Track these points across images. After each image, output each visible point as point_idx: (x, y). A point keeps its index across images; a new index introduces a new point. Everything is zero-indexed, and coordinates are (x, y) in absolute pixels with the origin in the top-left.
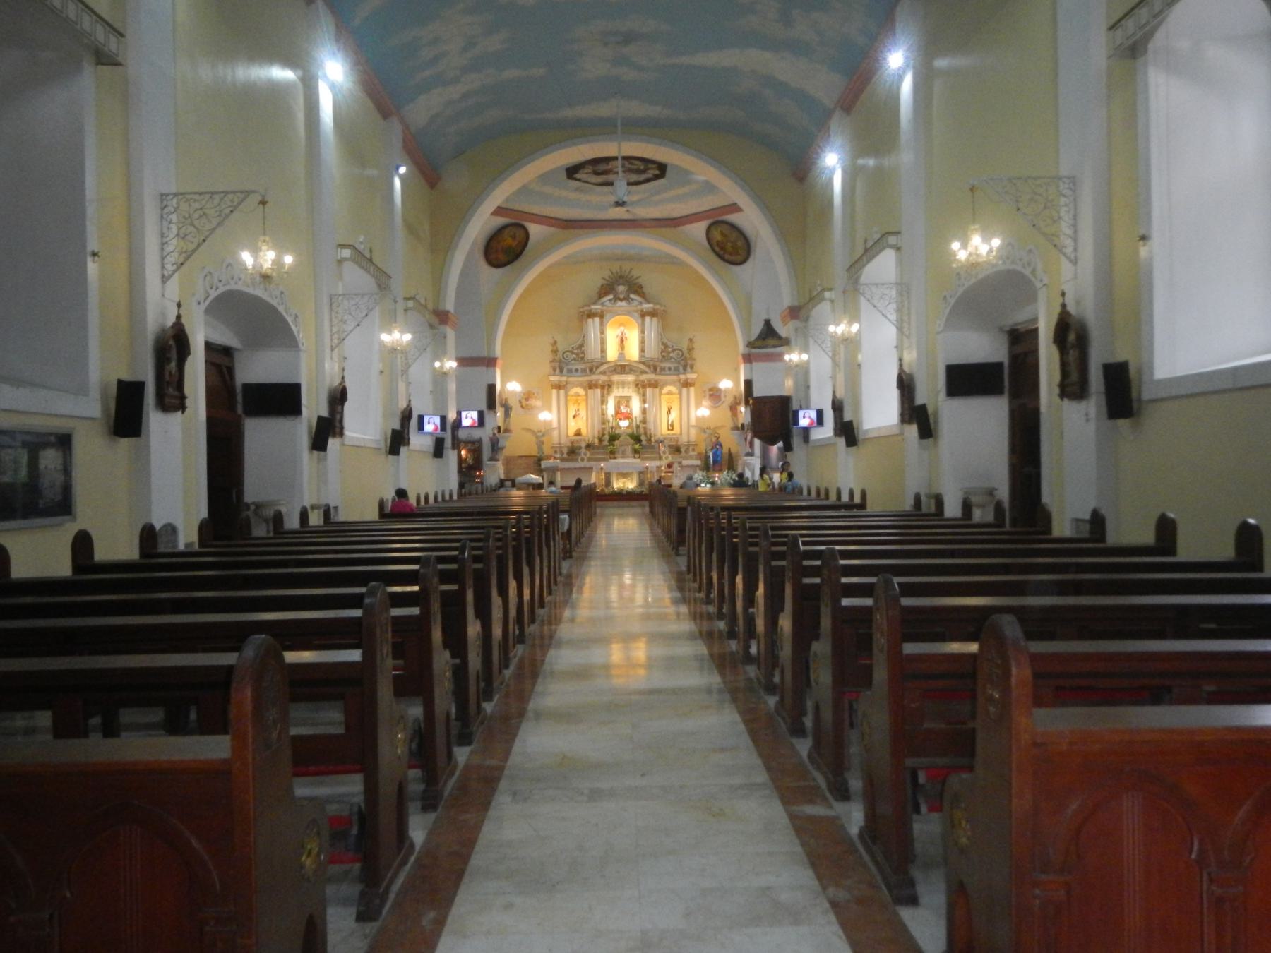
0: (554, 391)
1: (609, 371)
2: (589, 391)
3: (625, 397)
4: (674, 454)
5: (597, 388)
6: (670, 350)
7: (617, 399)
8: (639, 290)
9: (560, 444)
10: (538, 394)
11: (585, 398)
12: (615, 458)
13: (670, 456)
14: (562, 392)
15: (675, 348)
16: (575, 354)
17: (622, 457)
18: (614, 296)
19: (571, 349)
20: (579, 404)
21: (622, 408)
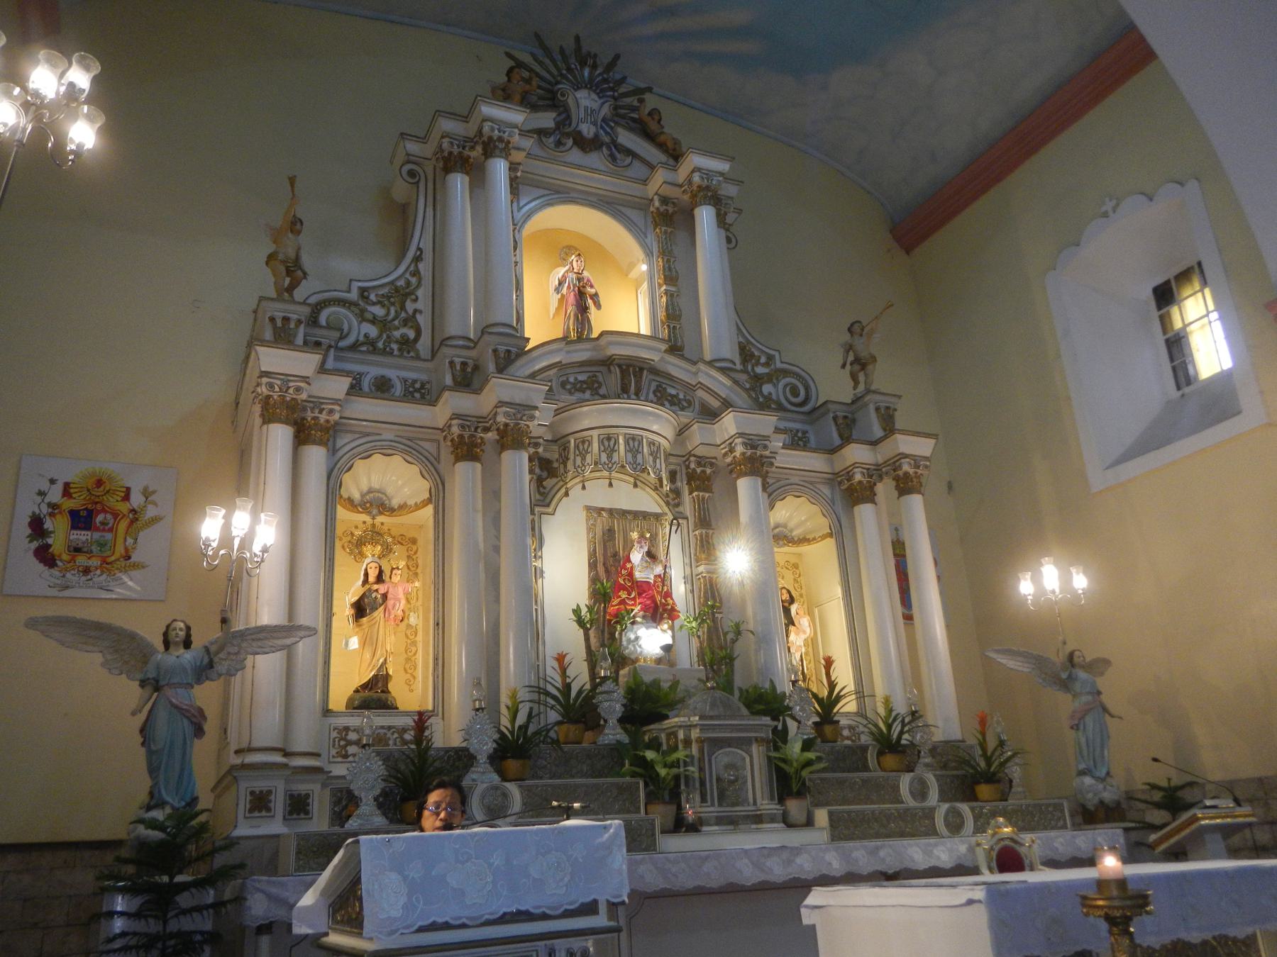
0: (280, 435)
1: (563, 385)
2: (462, 467)
3: (636, 515)
4: (976, 799)
5: (518, 445)
6: (760, 370)
7: (602, 523)
8: (653, 126)
9: (287, 754)
10: (147, 493)
11: (429, 510)
12: (680, 825)
13: (964, 808)
14: (315, 456)
15: (779, 365)
16: (374, 321)
17: (720, 821)
18: (559, 125)
19: (354, 295)
20: (387, 550)
21: (637, 557)
